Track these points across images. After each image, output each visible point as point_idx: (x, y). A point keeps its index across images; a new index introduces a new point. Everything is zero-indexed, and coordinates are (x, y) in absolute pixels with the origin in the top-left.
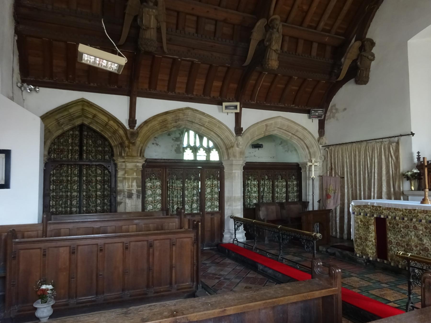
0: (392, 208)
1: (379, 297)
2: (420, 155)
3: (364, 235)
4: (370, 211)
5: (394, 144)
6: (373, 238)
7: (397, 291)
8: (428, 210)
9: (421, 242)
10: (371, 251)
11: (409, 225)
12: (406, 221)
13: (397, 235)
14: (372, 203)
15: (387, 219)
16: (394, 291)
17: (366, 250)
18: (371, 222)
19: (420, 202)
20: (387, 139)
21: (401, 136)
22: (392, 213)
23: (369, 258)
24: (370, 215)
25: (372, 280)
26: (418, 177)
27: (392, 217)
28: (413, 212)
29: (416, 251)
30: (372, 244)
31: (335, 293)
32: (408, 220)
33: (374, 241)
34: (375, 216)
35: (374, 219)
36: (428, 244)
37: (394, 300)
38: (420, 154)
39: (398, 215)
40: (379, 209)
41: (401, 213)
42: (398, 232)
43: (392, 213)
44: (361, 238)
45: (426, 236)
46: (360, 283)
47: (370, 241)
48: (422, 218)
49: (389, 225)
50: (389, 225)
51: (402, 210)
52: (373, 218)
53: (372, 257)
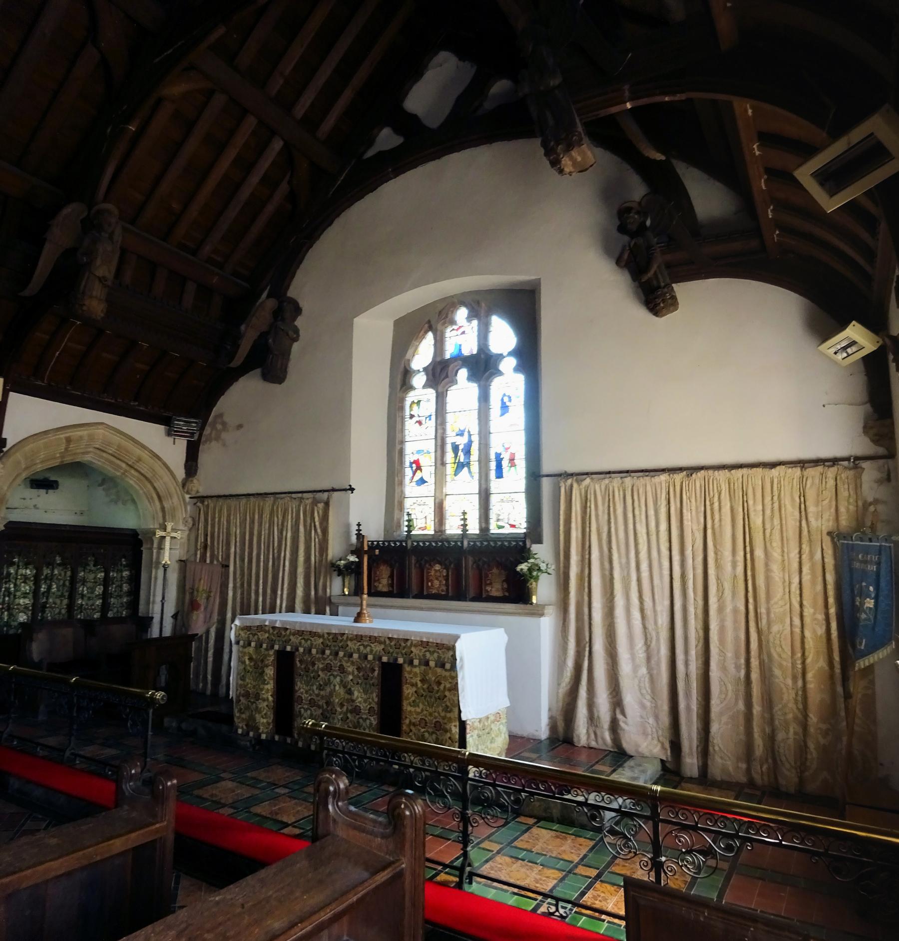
0: (307, 631)
1: (269, 818)
2: (361, 528)
3: (254, 687)
4: (268, 637)
5: (321, 505)
6: (270, 694)
7: (303, 800)
8: (363, 634)
9: (349, 697)
10: (265, 721)
11: (333, 665)
12: (328, 656)
13: (312, 685)
14: (272, 621)
15: (297, 653)
16: (296, 801)
17: (255, 720)
18: (268, 660)
19: (352, 619)
20: (310, 495)
21: (334, 490)
22: (306, 640)
23: (260, 735)
24: (267, 646)
25: (262, 781)
26: (353, 570)
27: (304, 650)
28: (340, 638)
29: (340, 714)
30: (267, 706)
31: (158, 836)
32: (331, 654)
33: (271, 699)
34: (276, 647)
35: (274, 653)
36: (360, 699)
37: (293, 820)
38: (361, 528)
39: (316, 645)
40: (283, 633)
41: (321, 640)
42: (314, 678)
43: (306, 640)
44: (247, 695)
45: (358, 684)
46: (236, 792)
47: (264, 700)
48: (354, 649)
49: (298, 664)
50: (298, 664)
51: (321, 634)
52: (271, 652)
53: (266, 733)
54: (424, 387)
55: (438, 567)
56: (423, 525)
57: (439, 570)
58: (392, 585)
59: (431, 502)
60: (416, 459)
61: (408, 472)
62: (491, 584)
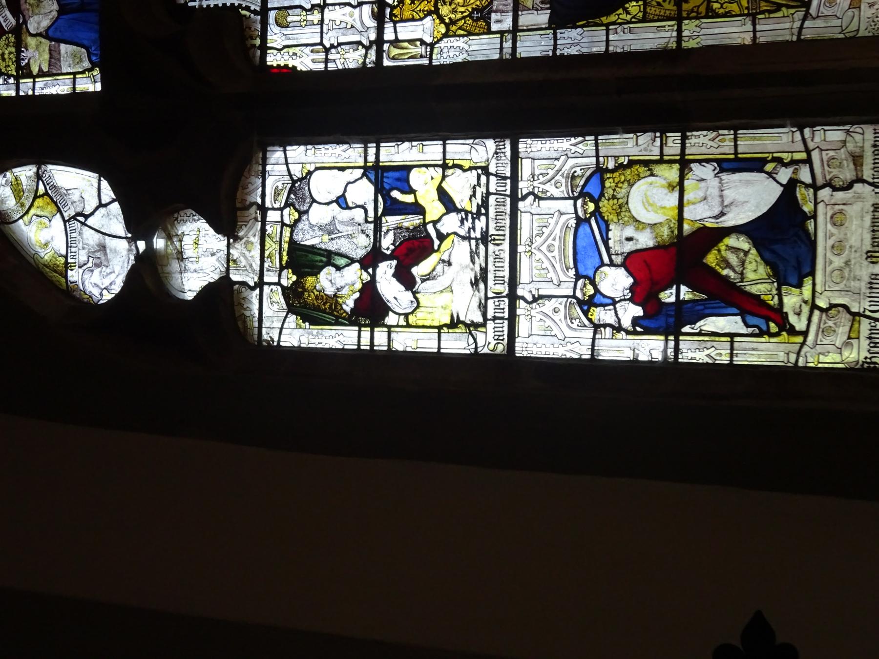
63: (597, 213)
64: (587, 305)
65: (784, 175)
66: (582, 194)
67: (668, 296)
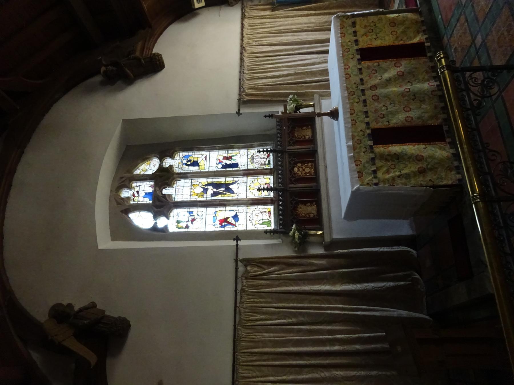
54: (168, 218)
55: (296, 169)
56: (267, 214)
57: (298, 169)
58: (311, 202)
59: (251, 209)
60: (219, 222)
61: (229, 228)
62: (304, 136)
63: (216, 216)
64: (214, 225)
65: (236, 212)
66: (214, 214)
67: (223, 224)
